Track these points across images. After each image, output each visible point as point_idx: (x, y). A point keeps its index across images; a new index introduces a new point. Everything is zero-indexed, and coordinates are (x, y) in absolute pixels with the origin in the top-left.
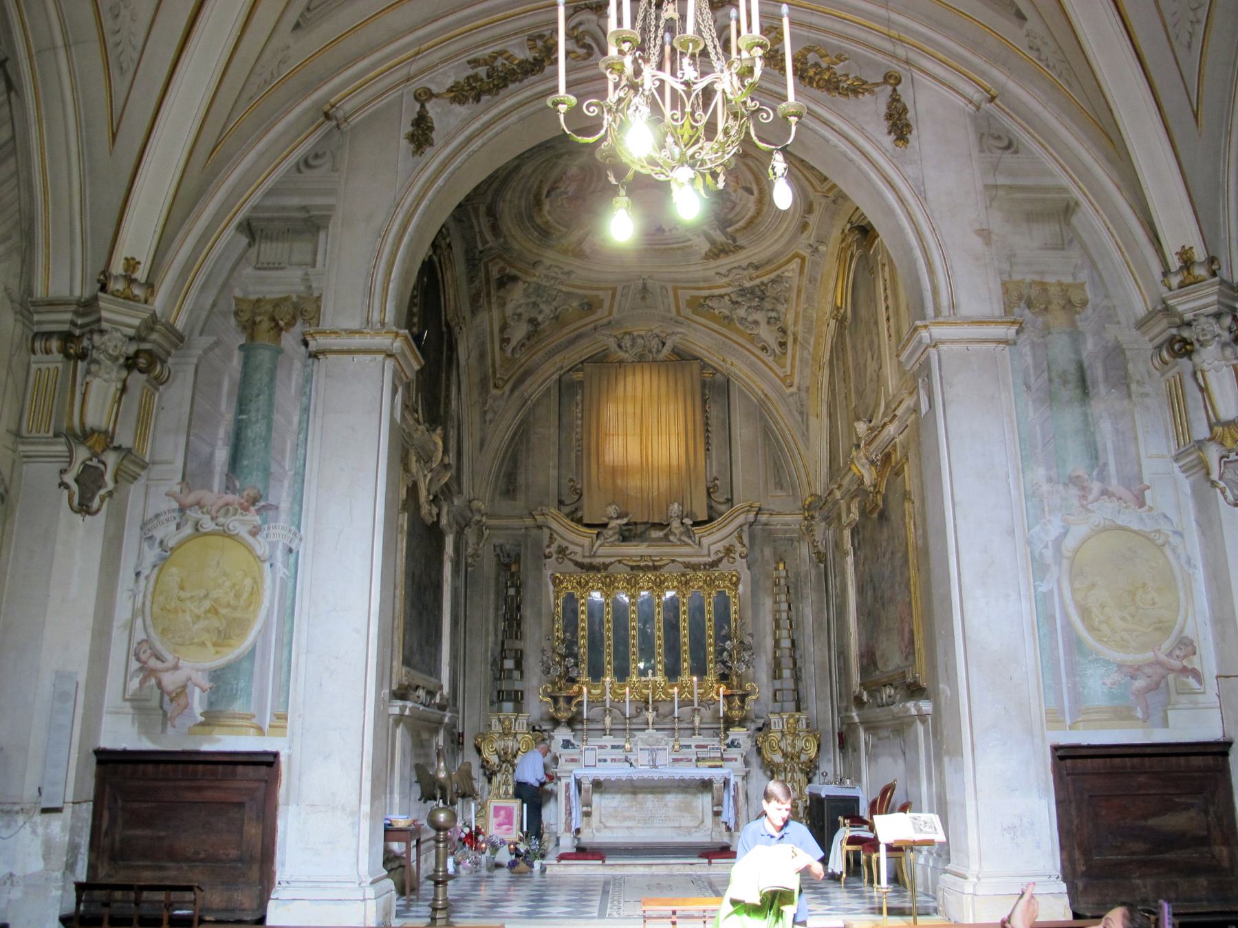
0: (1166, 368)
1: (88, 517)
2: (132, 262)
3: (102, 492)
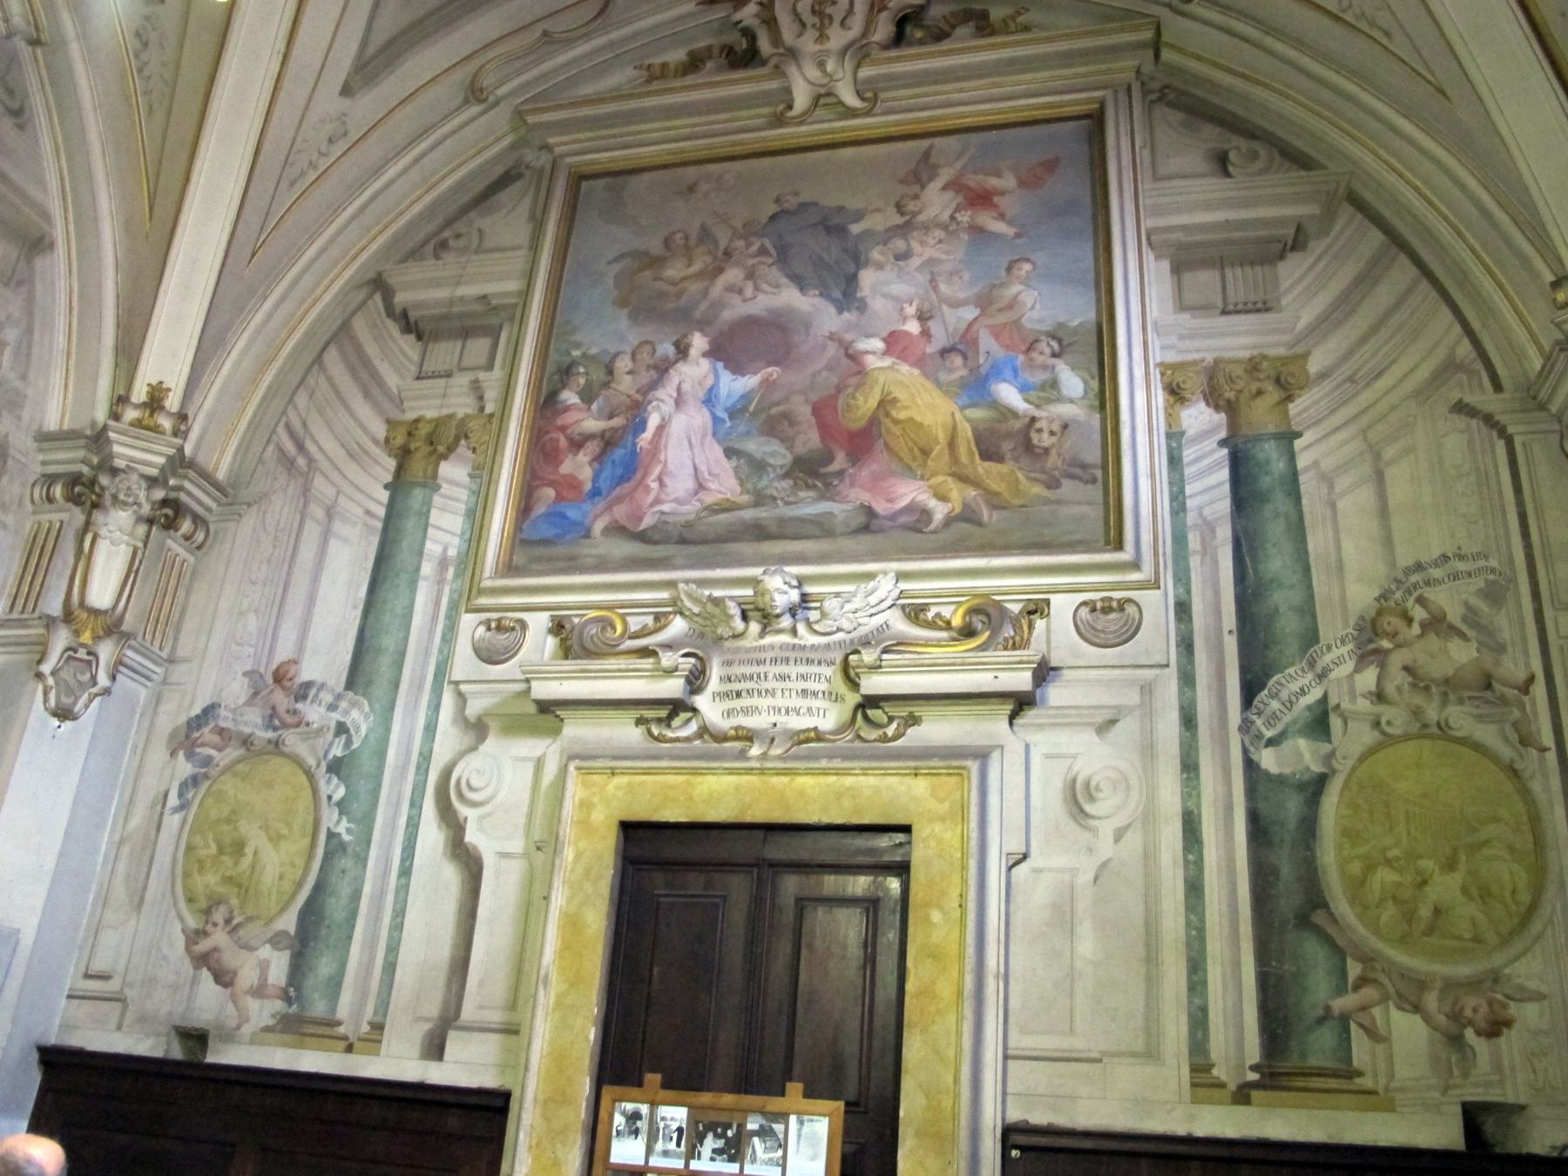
0: (47, 506)
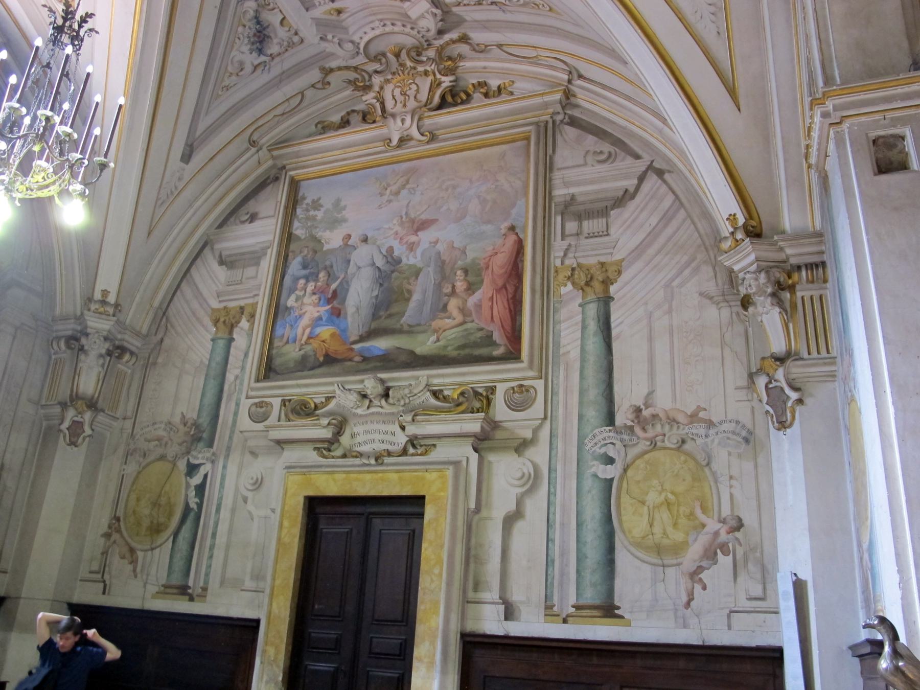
1: (788, 430)
2: (732, 218)
3: (789, 404)
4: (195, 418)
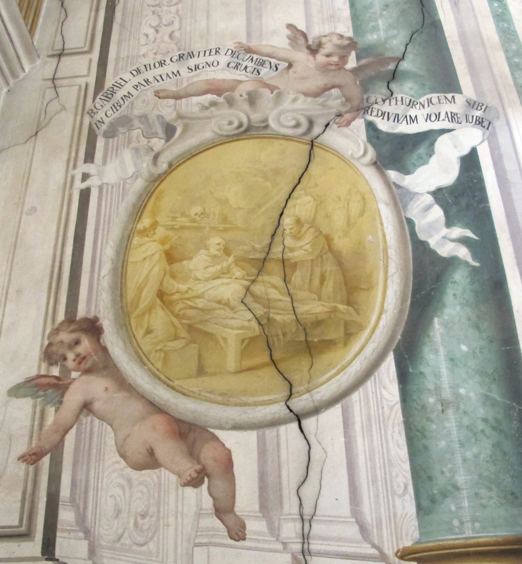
4: (350, 34)
